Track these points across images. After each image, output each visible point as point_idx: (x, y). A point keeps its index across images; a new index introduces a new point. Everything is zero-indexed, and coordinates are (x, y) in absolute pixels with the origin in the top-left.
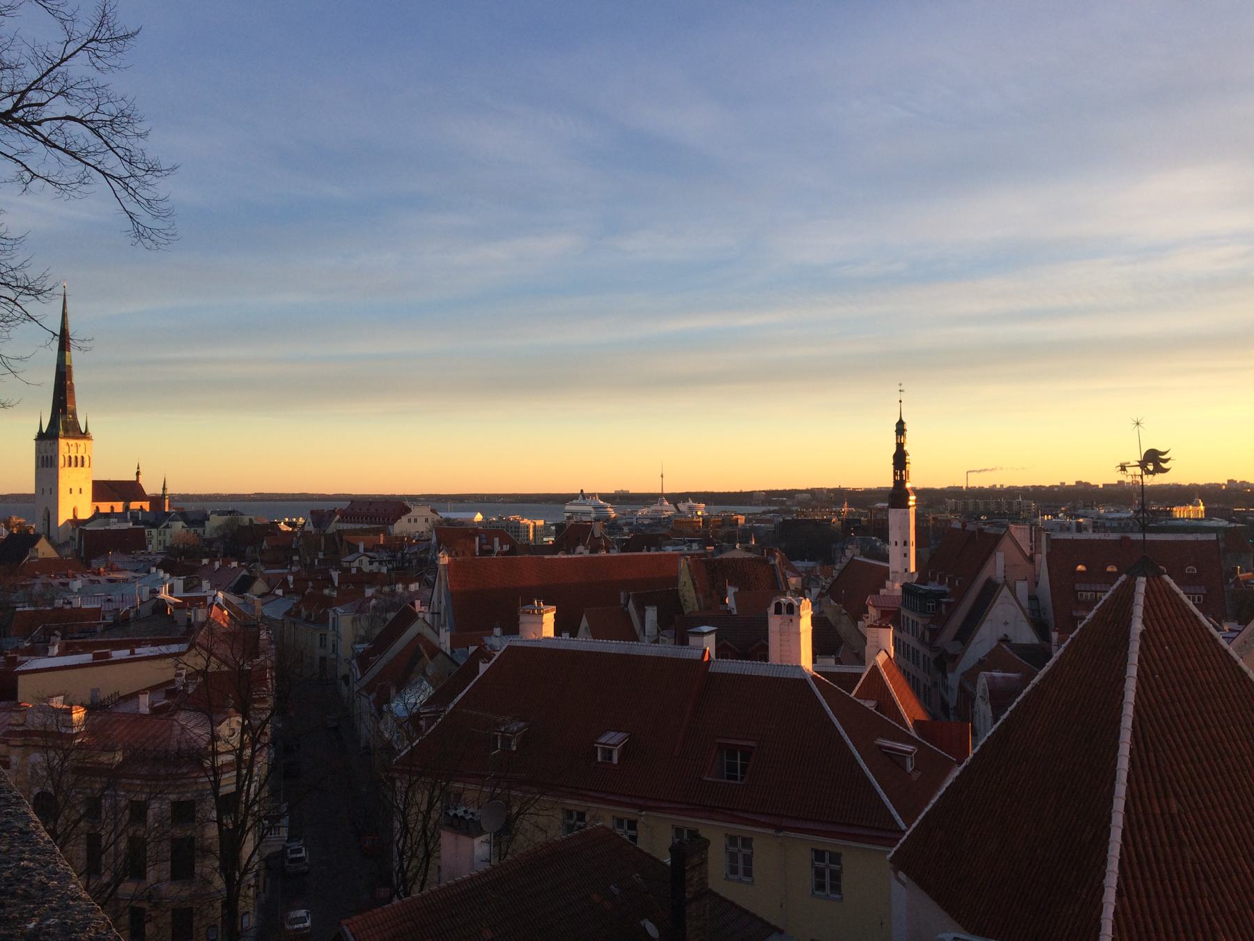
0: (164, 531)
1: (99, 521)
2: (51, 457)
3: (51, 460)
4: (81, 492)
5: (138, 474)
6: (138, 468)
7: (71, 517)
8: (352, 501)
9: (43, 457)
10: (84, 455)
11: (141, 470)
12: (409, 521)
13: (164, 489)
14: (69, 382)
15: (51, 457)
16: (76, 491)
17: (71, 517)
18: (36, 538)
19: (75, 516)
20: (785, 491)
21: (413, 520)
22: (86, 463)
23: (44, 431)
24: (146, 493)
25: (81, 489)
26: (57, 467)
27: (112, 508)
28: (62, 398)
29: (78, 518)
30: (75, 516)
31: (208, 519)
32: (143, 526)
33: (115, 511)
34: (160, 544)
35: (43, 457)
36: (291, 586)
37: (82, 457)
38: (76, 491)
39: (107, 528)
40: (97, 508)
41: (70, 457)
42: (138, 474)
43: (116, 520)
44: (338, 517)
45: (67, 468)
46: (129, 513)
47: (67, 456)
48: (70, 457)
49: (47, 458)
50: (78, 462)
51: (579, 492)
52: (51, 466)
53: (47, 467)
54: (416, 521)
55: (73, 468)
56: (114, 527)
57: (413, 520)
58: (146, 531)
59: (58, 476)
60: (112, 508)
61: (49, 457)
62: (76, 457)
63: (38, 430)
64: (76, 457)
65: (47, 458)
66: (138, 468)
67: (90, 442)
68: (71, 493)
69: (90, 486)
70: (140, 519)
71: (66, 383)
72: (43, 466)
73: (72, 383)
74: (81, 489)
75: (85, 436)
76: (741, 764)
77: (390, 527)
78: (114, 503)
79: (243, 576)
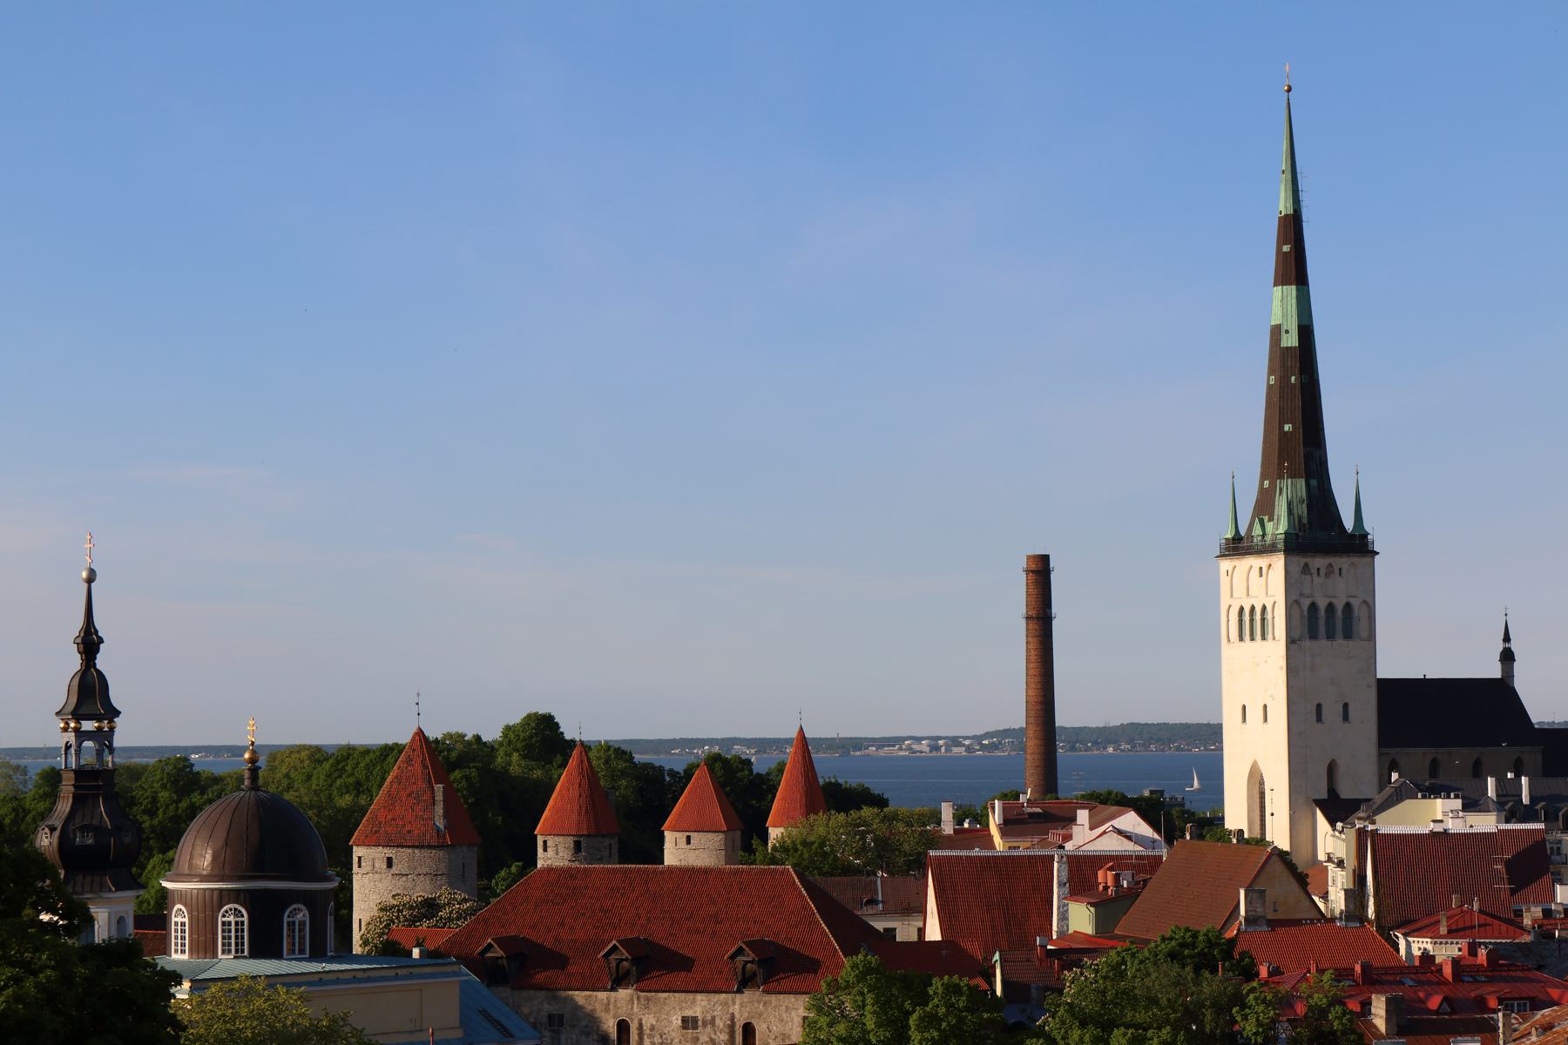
1: (1408, 804)
2: (1264, 608)
4: (1346, 718)
5: (1507, 657)
6: (1507, 639)
7: (1324, 795)
9: (1242, 609)
10: (1352, 601)
11: (1514, 646)
15: (1264, 608)
16: (1332, 713)
17: (1324, 795)
19: (1332, 791)
20: (149, 747)
23: (1243, 533)
24: (1534, 720)
25: (1346, 706)
28: (1287, 427)
30: (1332, 791)
35: (1242, 609)
37: (1348, 606)
38: (1332, 713)
39: (1439, 828)
41: (1313, 607)
42: (1507, 657)
43: (1458, 804)
45: (1307, 643)
46: (1491, 782)
47: (1306, 603)
48: (1313, 607)
49: (1253, 608)
51: (794, 734)
55: (1324, 643)
56: (1454, 826)
62: (1331, 607)
64: (1331, 607)
65: (1253, 608)
66: (1507, 639)
67: (1366, 560)
68: (1319, 718)
69: (1371, 696)
72: (1241, 639)
74: (1346, 706)
75: (1359, 545)
76: (299, 954)
78: (1441, 750)
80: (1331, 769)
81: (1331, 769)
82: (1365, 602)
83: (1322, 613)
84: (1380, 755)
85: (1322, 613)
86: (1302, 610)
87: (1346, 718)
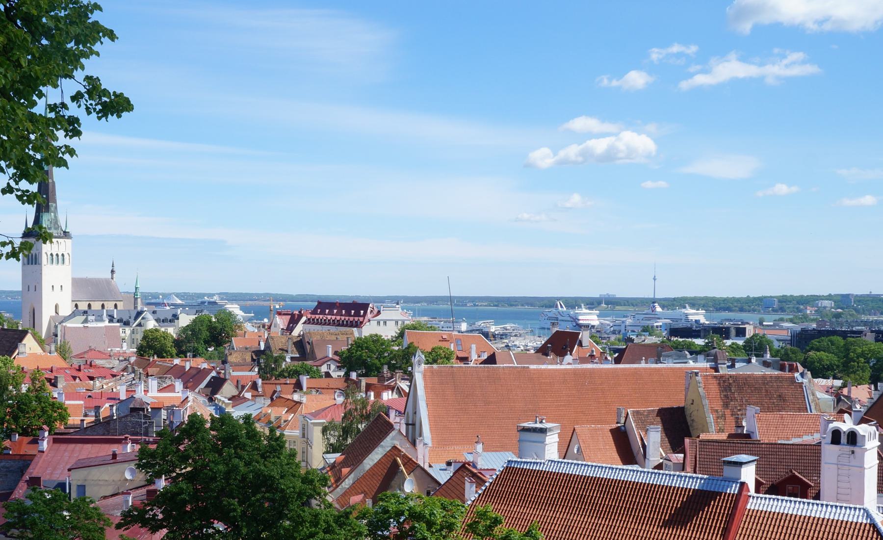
0: (137, 329)
3: (36, 258)
4: (62, 289)
8: (319, 303)
12: (379, 323)
13: (136, 288)
14: (50, 181)
16: (57, 288)
17: (54, 314)
18: (24, 333)
21: (382, 323)
22: (67, 261)
26: (40, 264)
27: (89, 306)
29: (60, 315)
31: (178, 319)
32: (118, 324)
33: (92, 308)
34: (133, 343)
36: (260, 390)
37: (63, 255)
38: (57, 288)
40: (76, 306)
41: (52, 255)
42: (113, 272)
43: (93, 318)
44: (304, 319)
45: (49, 265)
47: (49, 254)
50: (57, 259)
52: (36, 264)
53: (32, 264)
54: (385, 323)
57: (382, 323)
58: (121, 330)
59: (41, 274)
60: (89, 306)
61: (34, 255)
62: (57, 255)
63: (23, 229)
70: (115, 317)
71: (48, 181)
72: (28, 264)
73: (54, 183)
77: (355, 329)
79: (213, 377)
80: (56, 307)
81: (56, 307)
82: (68, 254)
83: (55, 257)
84: (72, 301)
85: (55, 257)
86: (47, 256)
87: (62, 289)
